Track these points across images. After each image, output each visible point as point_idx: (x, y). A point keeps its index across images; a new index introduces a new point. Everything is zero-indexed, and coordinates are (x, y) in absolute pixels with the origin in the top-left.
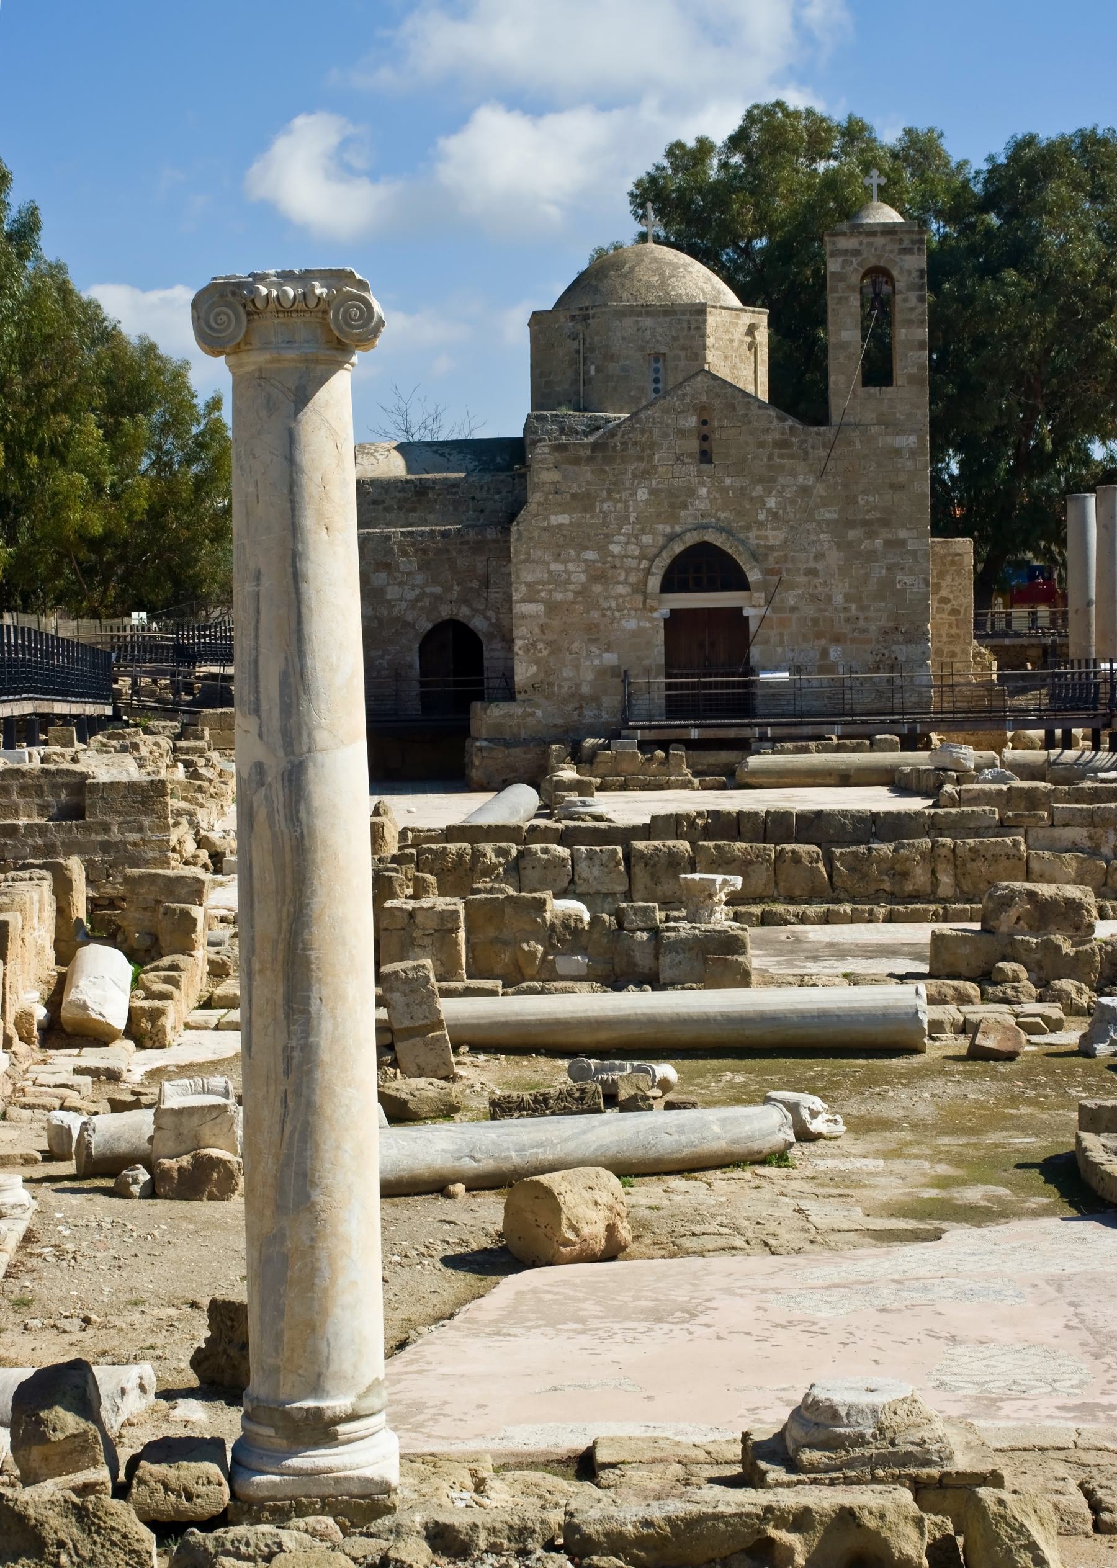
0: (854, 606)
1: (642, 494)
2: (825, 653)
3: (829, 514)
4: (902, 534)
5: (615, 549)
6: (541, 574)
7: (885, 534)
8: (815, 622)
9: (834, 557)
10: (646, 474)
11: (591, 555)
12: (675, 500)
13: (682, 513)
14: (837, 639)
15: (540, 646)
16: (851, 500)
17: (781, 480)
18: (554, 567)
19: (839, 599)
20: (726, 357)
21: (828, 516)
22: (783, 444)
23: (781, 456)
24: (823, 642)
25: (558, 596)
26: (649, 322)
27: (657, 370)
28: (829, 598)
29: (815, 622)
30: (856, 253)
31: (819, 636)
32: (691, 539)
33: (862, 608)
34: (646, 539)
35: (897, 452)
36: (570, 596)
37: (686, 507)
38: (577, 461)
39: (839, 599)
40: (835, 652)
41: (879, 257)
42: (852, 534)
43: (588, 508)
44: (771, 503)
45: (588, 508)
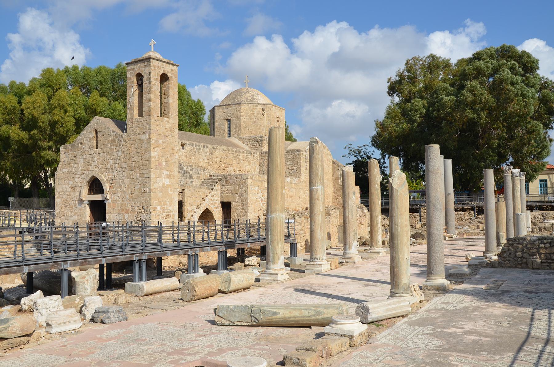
0: (131, 199)
1: (82, 161)
2: (124, 217)
3: (124, 165)
4: (144, 172)
5: (76, 180)
6: (61, 190)
7: (139, 172)
8: (122, 205)
9: (127, 181)
10: (83, 154)
11: (71, 182)
12: (89, 164)
13: (90, 167)
14: (127, 212)
15: (60, 213)
16: (131, 161)
17: (114, 153)
18: (64, 186)
19: (128, 197)
20: (251, 119)
21: (125, 166)
22: (114, 141)
23: (113, 145)
24: (123, 213)
25: (64, 197)
26: (226, 110)
27: (229, 124)
28: (125, 197)
29: (122, 205)
30: (133, 69)
31: (123, 210)
32: (91, 176)
33: (133, 200)
34: (83, 176)
35: (142, 142)
36: (67, 197)
37: (91, 165)
38: (68, 151)
39: (128, 197)
40: (127, 216)
41: (139, 70)
42: (131, 172)
43: (70, 167)
44: (111, 162)
45: (70, 167)
